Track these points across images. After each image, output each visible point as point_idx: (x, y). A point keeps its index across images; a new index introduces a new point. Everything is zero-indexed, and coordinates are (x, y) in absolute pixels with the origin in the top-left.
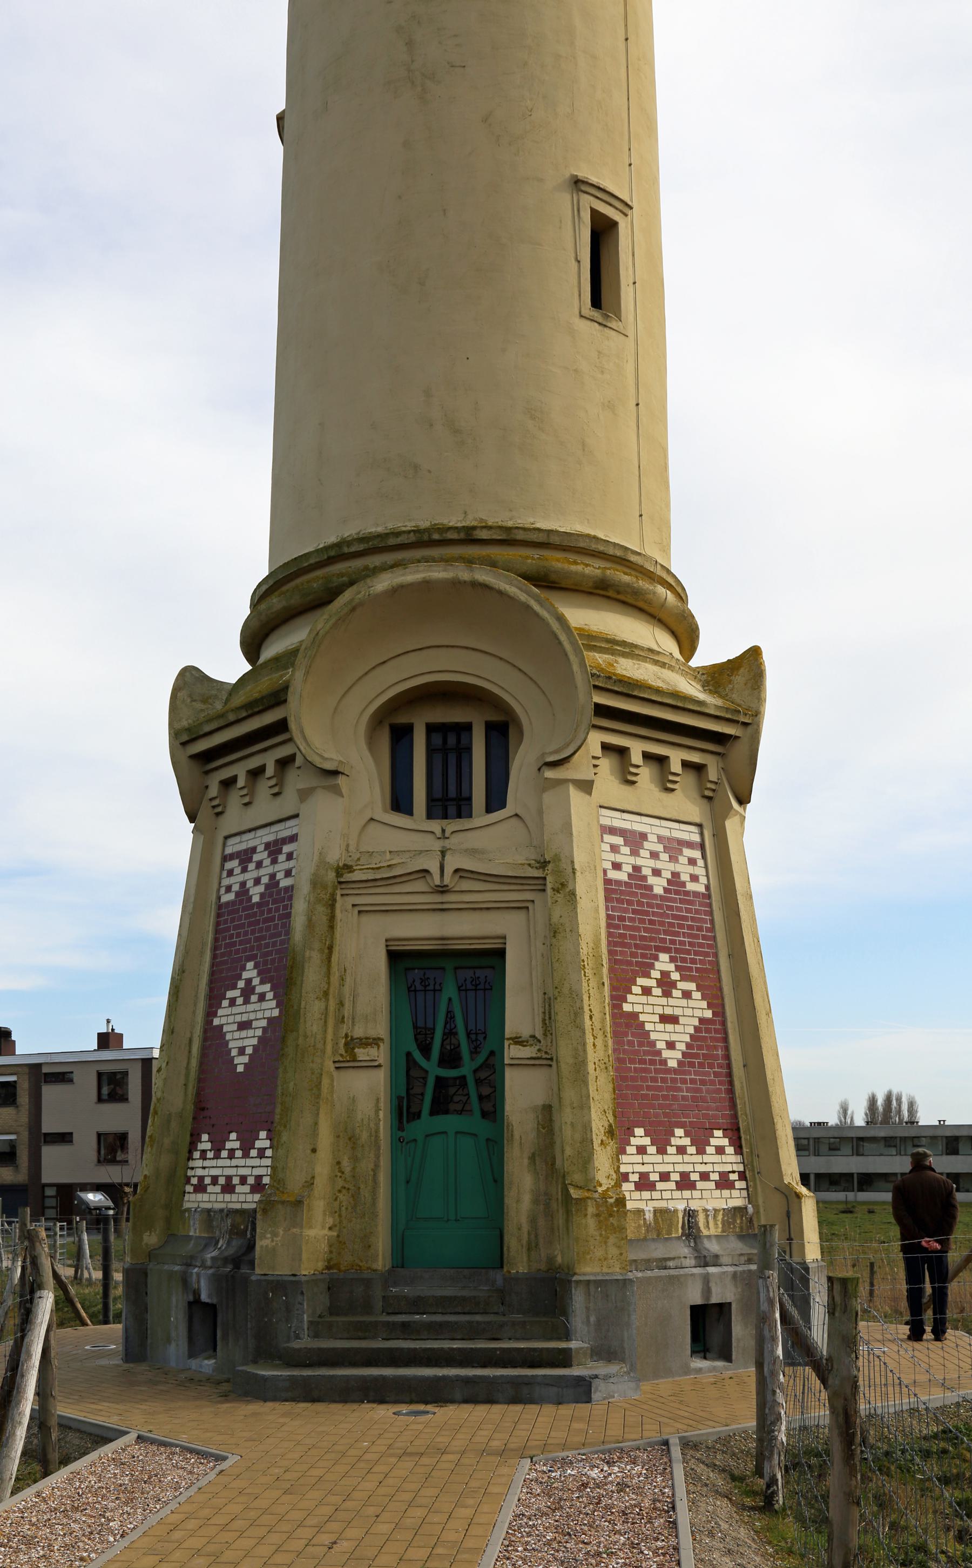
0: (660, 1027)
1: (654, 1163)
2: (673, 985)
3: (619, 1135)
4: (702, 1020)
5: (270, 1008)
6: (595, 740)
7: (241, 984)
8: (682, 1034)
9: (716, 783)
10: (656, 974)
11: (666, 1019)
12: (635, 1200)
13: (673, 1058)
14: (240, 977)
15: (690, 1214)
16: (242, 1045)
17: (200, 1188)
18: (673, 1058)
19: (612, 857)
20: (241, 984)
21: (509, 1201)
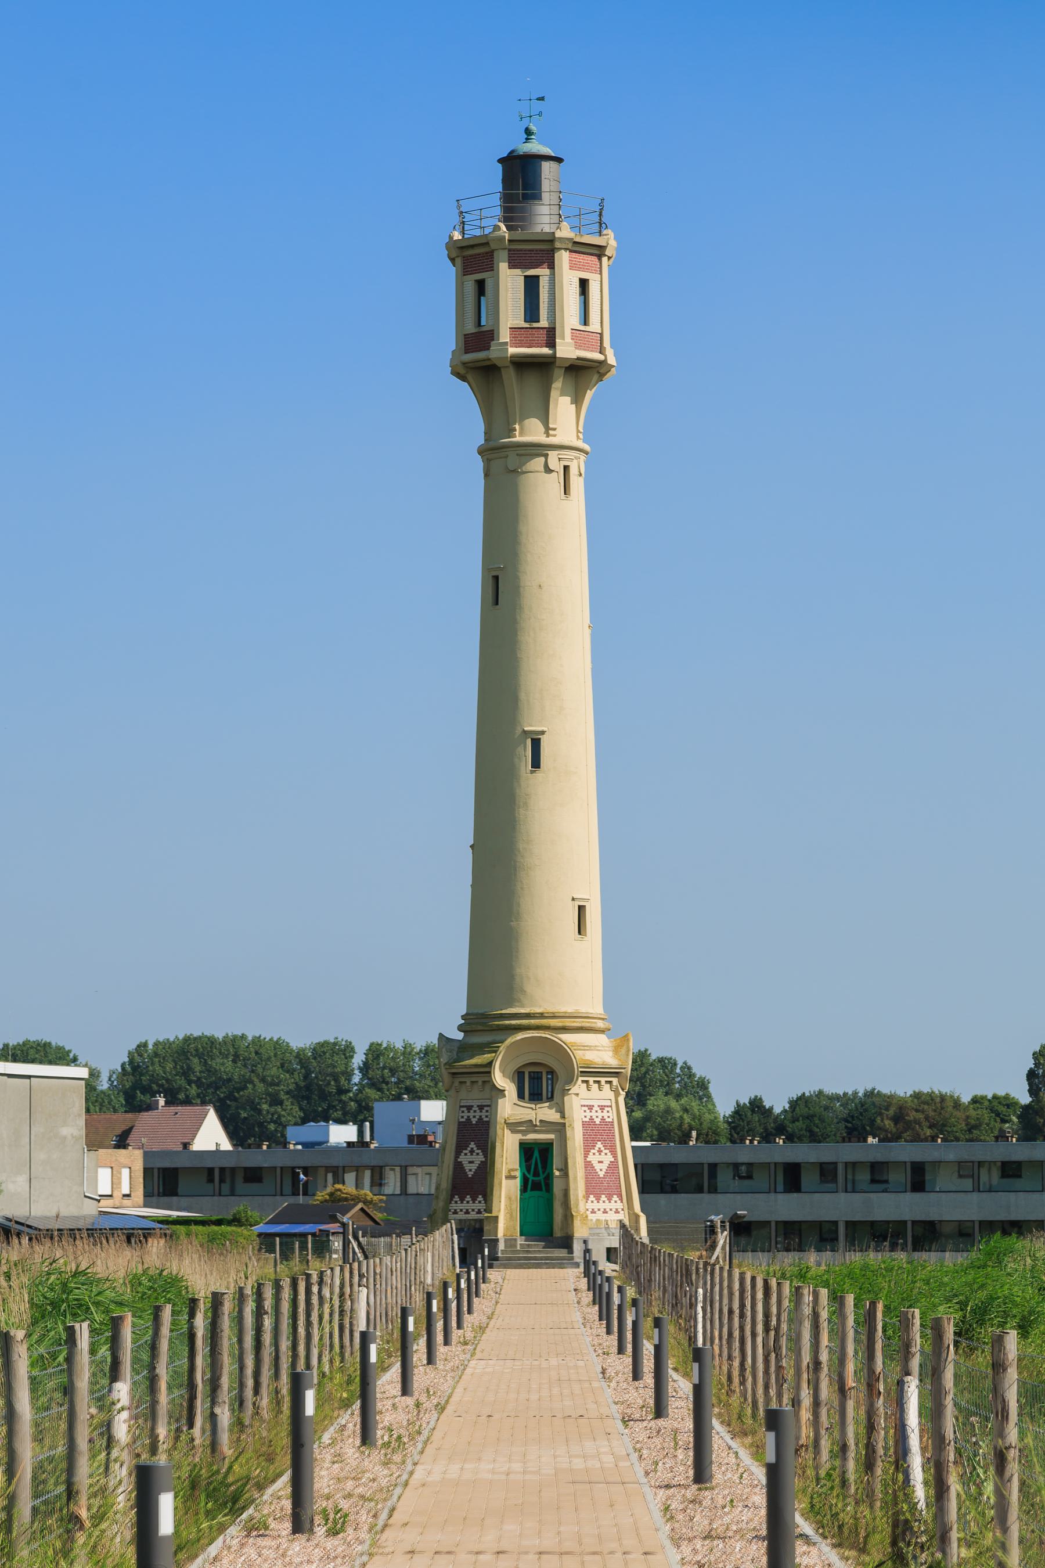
1: (596, 1206)
3: (587, 1198)
5: (481, 1158)
6: (581, 1079)
8: (604, 1166)
12: (591, 1216)
13: (601, 1174)
15: (607, 1221)
16: (470, 1169)
17: (455, 1212)
18: (601, 1174)
21: (555, 1216)
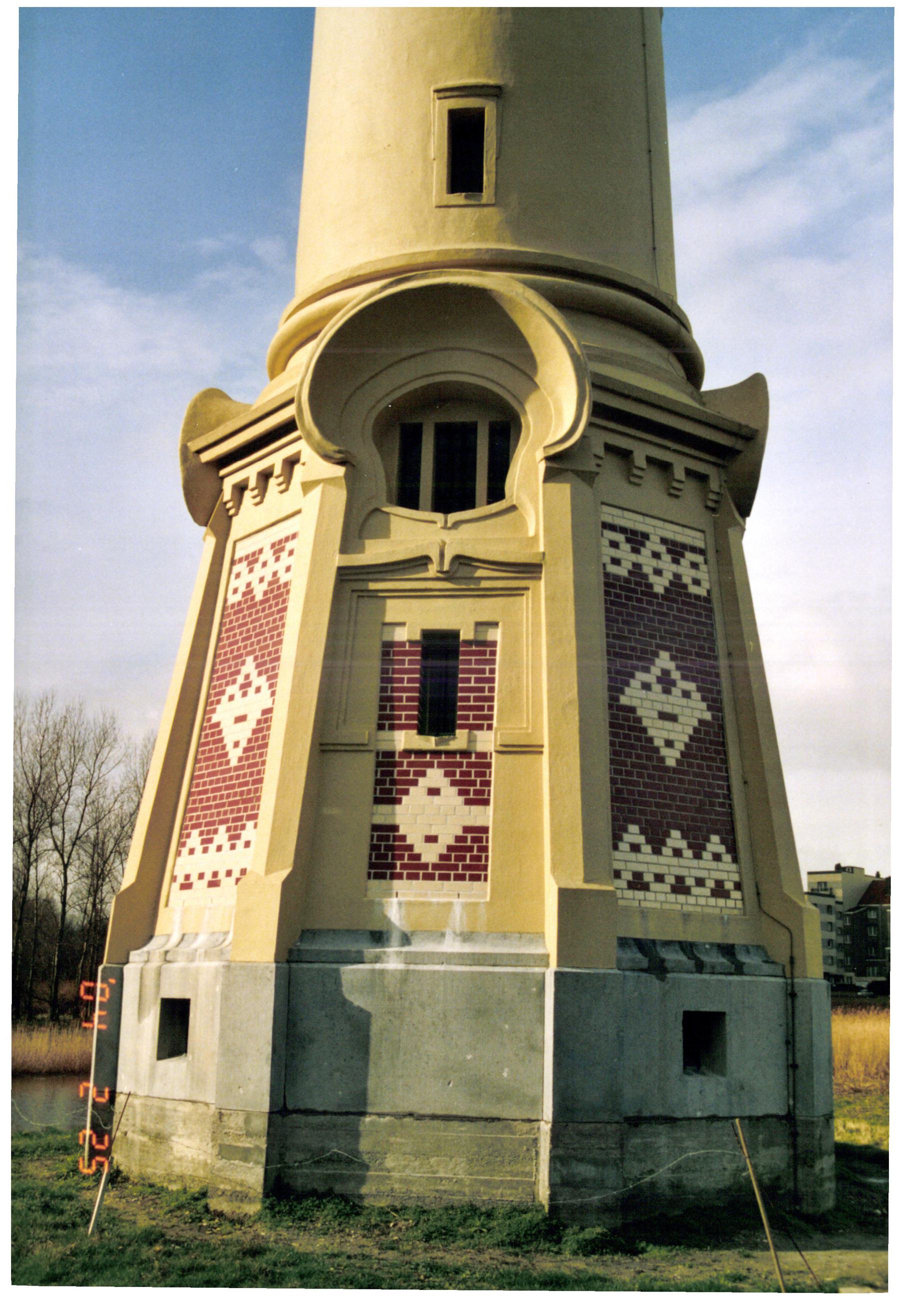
0: (660, 723)
1: (647, 862)
2: (673, 683)
4: (701, 721)
5: (264, 700)
7: (240, 679)
8: (681, 733)
9: (718, 494)
10: (656, 671)
11: (664, 716)
13: (671, 757)
14: (238, 672)
18: (671, 757)
19: (613, 552)
20: (240, 679)
